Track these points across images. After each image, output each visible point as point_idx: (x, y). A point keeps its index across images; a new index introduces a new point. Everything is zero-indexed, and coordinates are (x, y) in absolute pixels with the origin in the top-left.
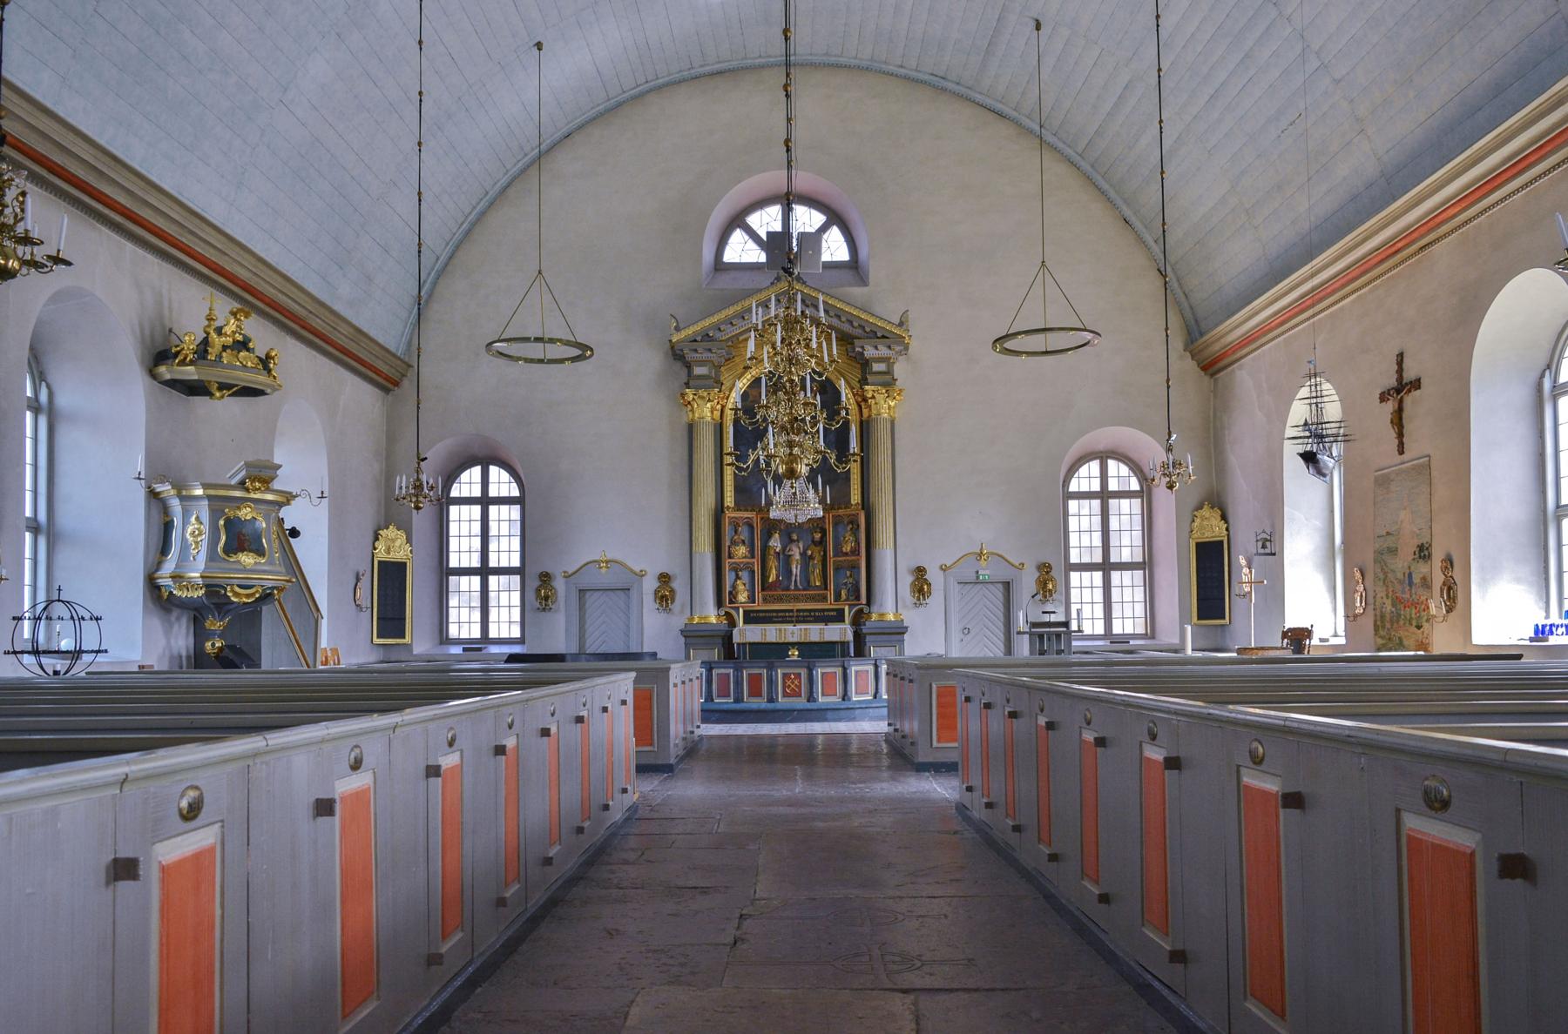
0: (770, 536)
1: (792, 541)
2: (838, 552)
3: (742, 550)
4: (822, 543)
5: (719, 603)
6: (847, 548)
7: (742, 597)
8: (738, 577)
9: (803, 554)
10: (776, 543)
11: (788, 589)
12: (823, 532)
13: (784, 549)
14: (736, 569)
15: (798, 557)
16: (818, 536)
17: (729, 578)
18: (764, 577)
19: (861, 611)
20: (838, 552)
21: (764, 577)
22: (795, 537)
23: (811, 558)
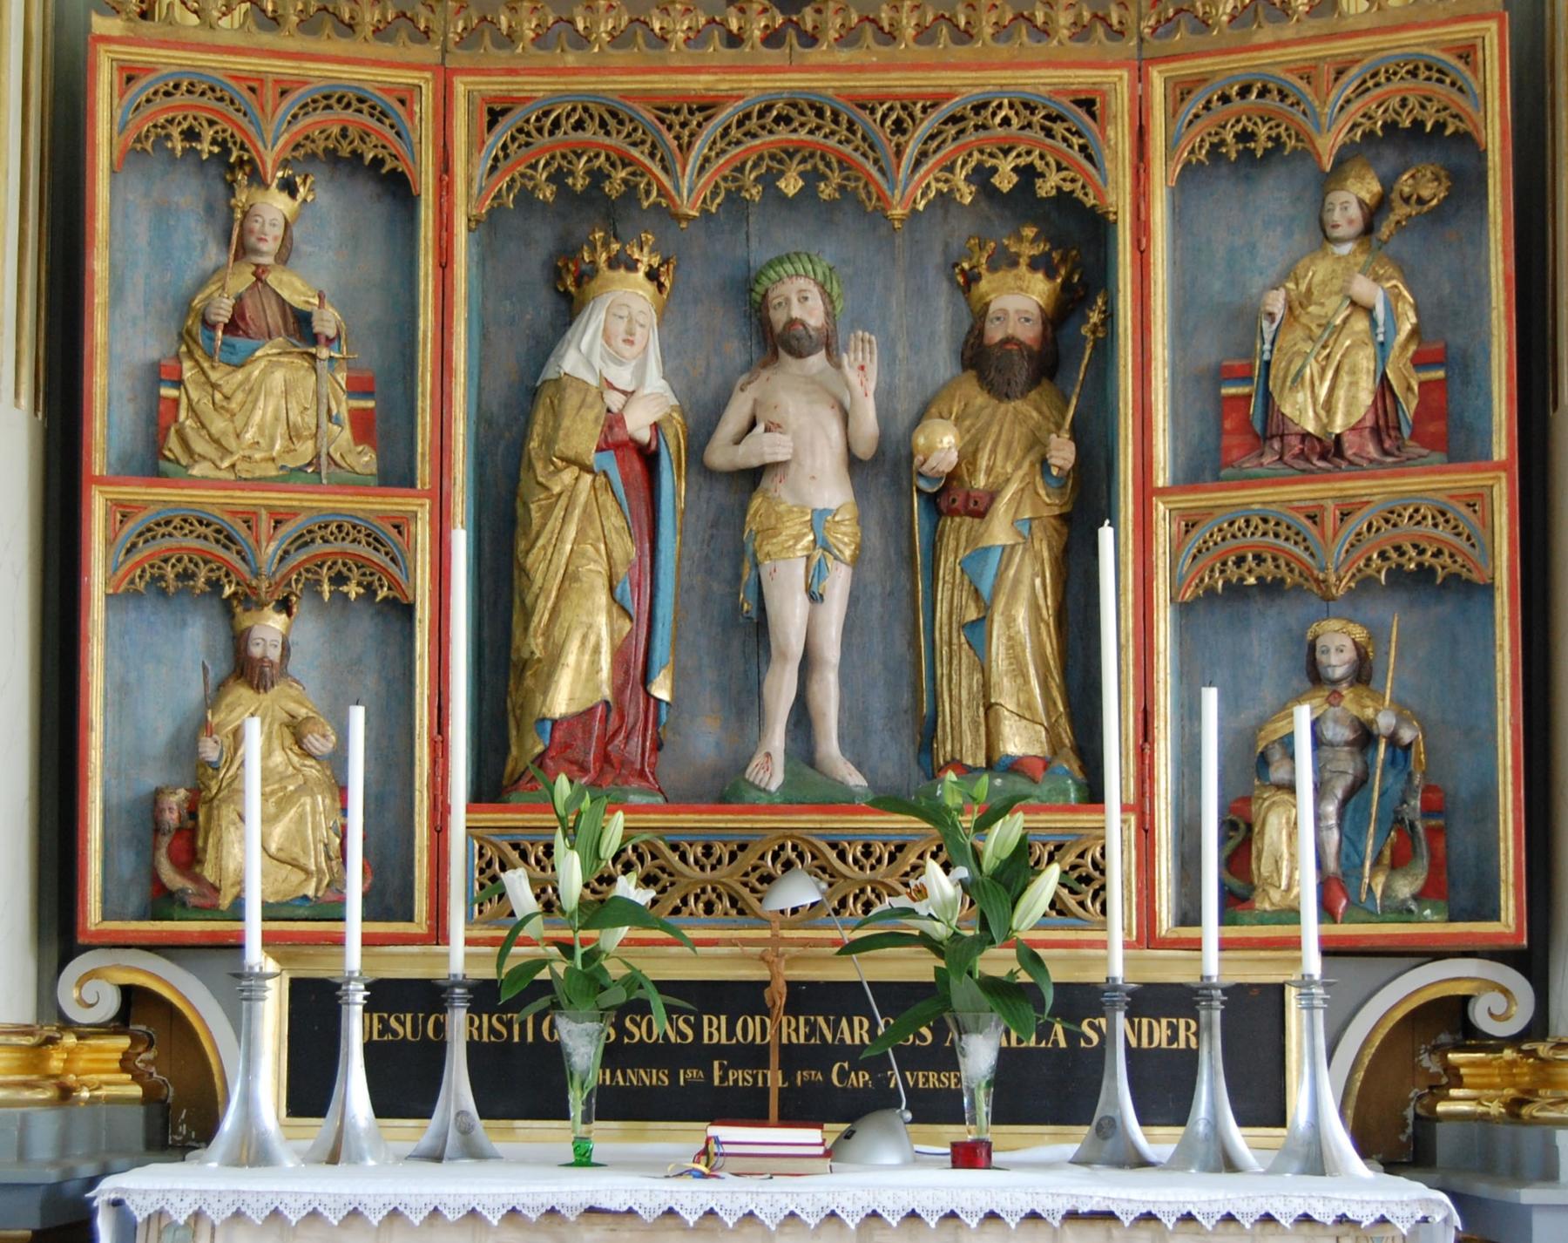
0: (569, 304)
1: (774, 342)
2: (1241, 422)
3: (275, 412)
4: (1065, 361)
5: (58, 929)
6: (1330, 392)
7: (250, 855)
8: (245, 669)
9: (882, 469)
10: (623, 357)
11: (728, 787)
12: (1080, 245)
13: (701, 423)
14: (208, 579)
15: (829, 489)
16: (1020, 301)
17: (138, 676)
18: (504, 670)
19: (1448, 1019)
20: (1241, 422)
21: (504, 670)
22: (801, 301)
23: (952, 499)
